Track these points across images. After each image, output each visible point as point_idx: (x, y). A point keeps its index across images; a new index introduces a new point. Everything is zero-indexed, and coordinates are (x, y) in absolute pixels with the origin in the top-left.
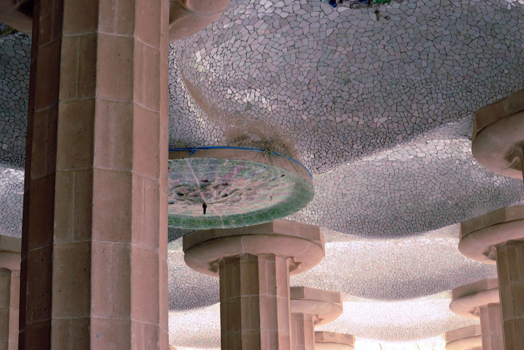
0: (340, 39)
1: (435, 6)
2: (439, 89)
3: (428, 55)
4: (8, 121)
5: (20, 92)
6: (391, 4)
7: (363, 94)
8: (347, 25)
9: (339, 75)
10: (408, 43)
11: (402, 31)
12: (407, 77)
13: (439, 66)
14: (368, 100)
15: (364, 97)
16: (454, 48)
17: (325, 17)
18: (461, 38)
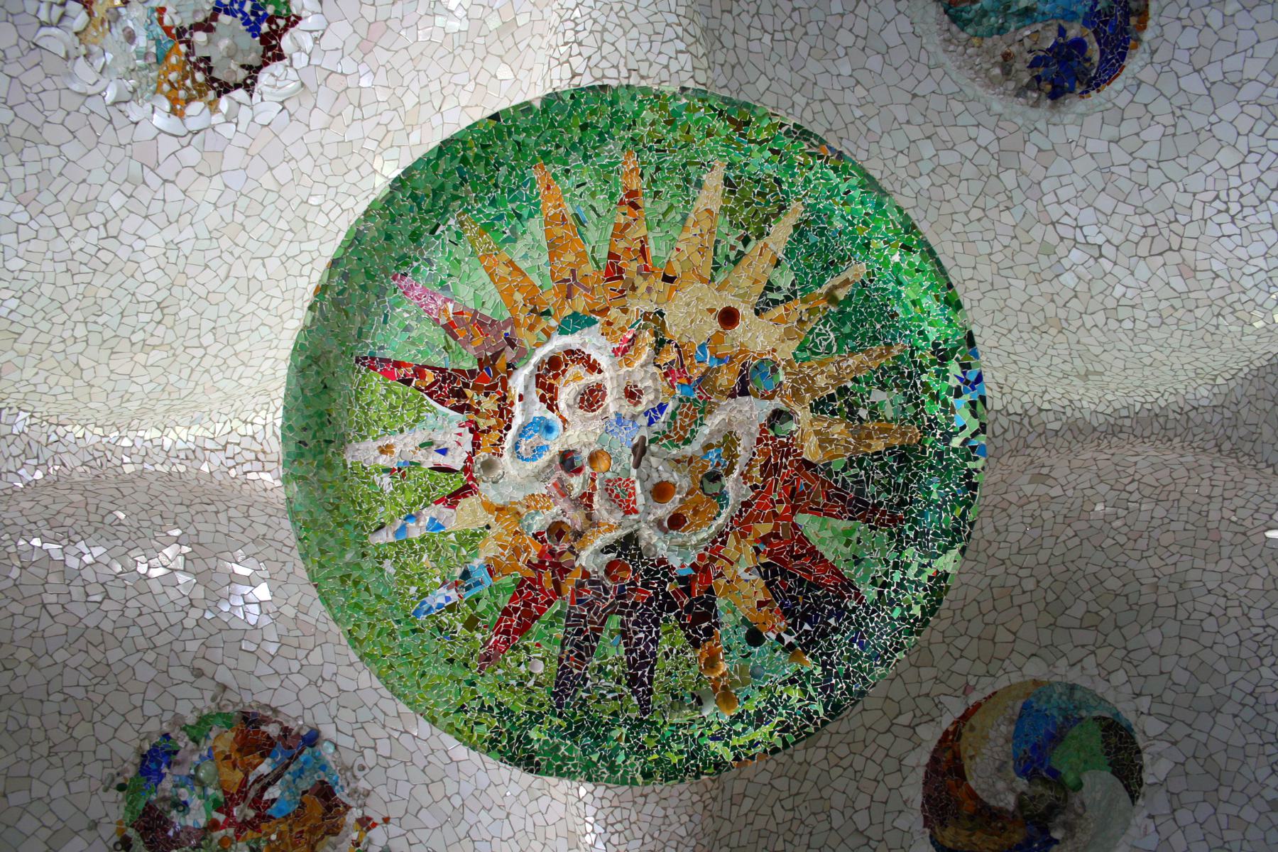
0: (292, 633)
1: (104, 717)
2: (30, 531)
3: (88, 595)
4: (1133, 481)
5: (1063, 538)
6: (196, 714)
7: (217, 513)
8: (279, 664)
9: (282, 557)
10: (141, 614)
11: (160, 640)
12: (119, 542)
13: (52, 578)
14: (198, 500)
15: (212, 508)
16: (33, 626)
17: (327, 699)
18: (23, 654)
